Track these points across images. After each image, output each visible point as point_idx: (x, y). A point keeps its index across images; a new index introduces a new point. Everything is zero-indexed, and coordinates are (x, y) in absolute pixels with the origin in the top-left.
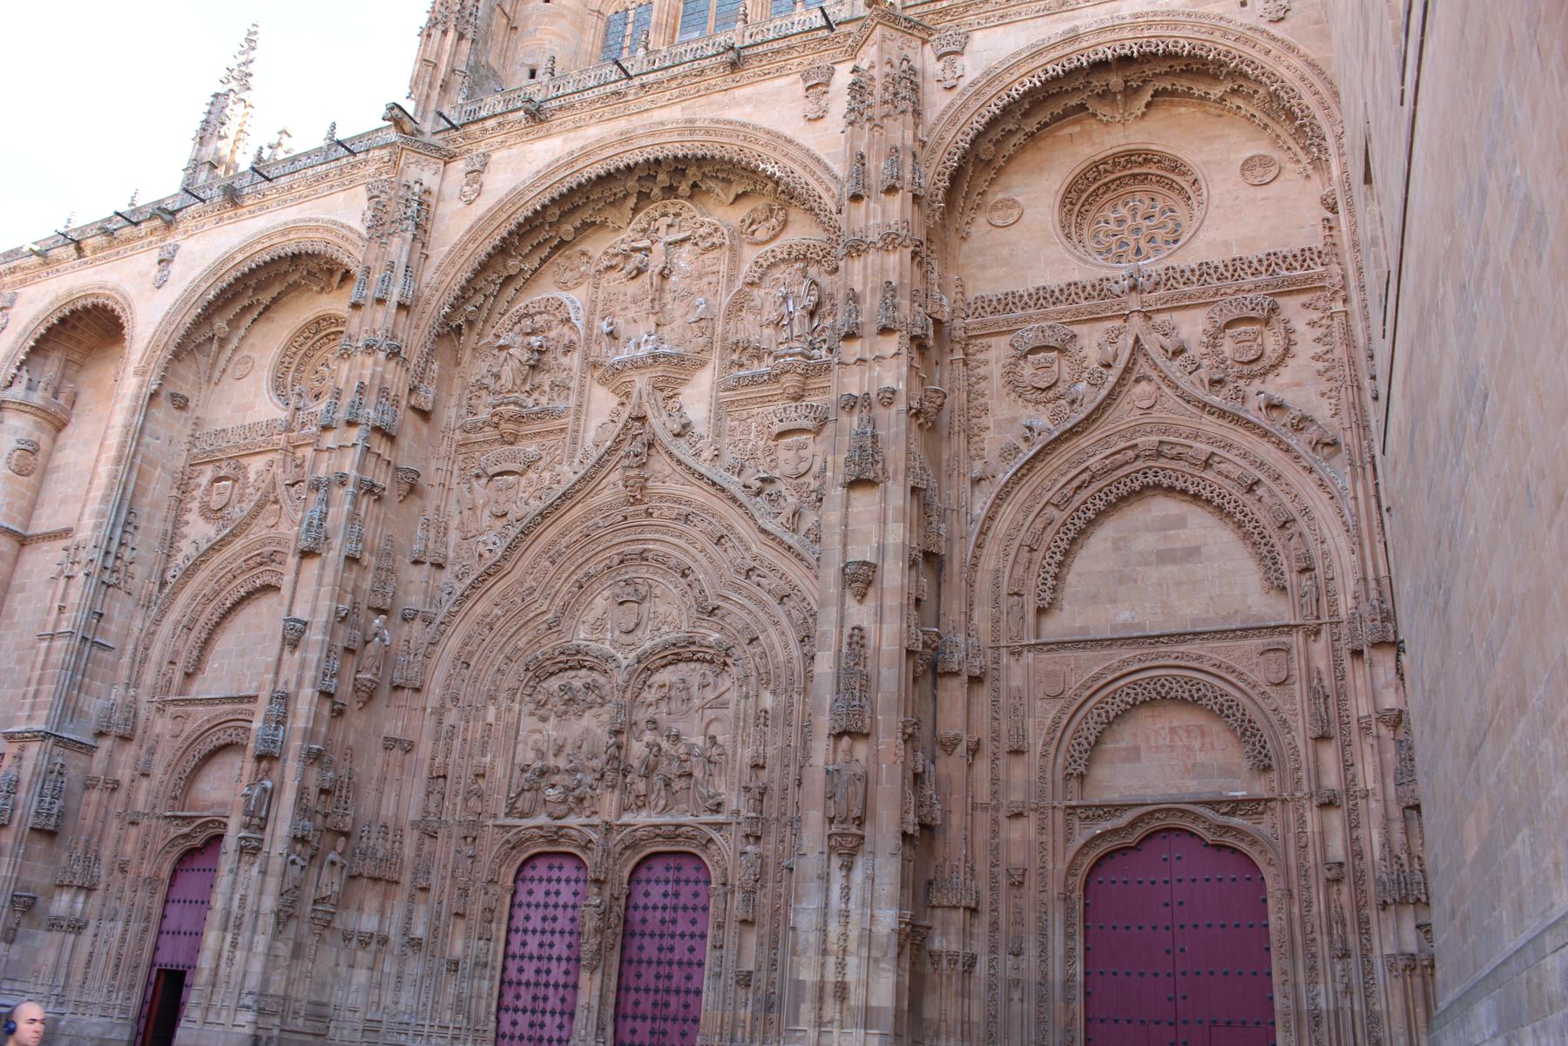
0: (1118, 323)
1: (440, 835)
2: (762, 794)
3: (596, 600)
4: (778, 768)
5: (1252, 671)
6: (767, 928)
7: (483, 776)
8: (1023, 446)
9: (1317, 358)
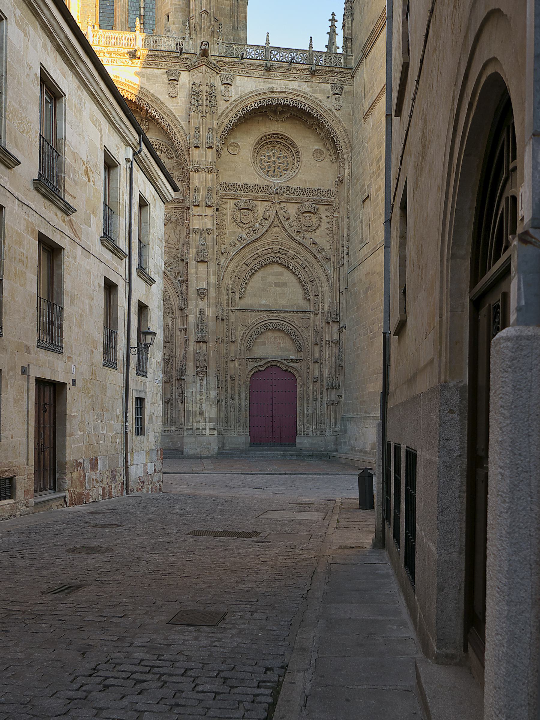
0: (270, 204)
5: (299, 323)
8: (237, 242)
9: (327, 229)
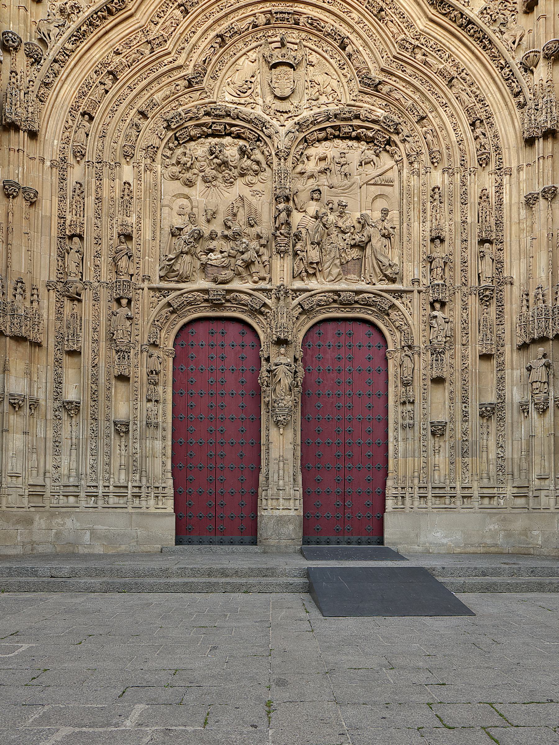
1: (82, 297)
2: (445, 263)
3: (240, 61)
4: (458, 242)
6: (459, 384)
7: (129, 237)
